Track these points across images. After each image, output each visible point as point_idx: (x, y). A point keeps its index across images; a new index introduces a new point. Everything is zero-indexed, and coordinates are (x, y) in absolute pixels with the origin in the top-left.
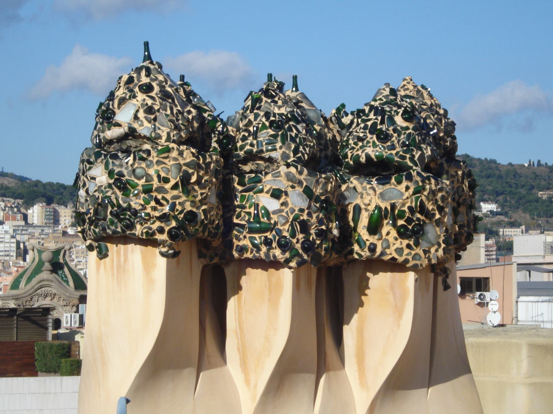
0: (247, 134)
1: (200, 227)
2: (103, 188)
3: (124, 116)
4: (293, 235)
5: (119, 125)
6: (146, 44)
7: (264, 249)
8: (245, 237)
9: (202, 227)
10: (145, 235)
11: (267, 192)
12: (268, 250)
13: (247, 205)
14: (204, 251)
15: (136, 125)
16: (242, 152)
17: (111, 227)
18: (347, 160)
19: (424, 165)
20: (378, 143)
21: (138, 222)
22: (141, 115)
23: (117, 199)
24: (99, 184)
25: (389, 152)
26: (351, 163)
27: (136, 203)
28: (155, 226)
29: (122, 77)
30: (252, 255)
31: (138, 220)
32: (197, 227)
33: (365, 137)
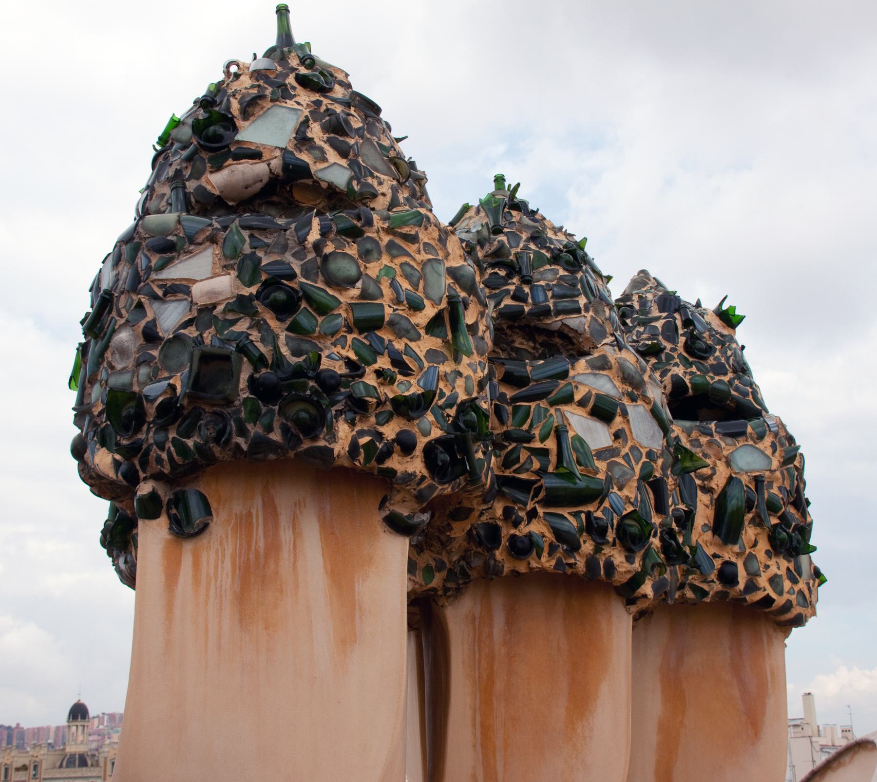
5: (256, 155)
7: (587, 547)
10: (361, 458)
11: (582, 403)
12: (598, 549)
13: (536, 432)
17: (249, 426)
20: (691, 359)
21: (340, 413)
22: (315, 131)
23: (270, 338)
24: (202, 301)
27: (333, 359)
28: (390, 431)
30: (553, 563)
31: (339, 407)
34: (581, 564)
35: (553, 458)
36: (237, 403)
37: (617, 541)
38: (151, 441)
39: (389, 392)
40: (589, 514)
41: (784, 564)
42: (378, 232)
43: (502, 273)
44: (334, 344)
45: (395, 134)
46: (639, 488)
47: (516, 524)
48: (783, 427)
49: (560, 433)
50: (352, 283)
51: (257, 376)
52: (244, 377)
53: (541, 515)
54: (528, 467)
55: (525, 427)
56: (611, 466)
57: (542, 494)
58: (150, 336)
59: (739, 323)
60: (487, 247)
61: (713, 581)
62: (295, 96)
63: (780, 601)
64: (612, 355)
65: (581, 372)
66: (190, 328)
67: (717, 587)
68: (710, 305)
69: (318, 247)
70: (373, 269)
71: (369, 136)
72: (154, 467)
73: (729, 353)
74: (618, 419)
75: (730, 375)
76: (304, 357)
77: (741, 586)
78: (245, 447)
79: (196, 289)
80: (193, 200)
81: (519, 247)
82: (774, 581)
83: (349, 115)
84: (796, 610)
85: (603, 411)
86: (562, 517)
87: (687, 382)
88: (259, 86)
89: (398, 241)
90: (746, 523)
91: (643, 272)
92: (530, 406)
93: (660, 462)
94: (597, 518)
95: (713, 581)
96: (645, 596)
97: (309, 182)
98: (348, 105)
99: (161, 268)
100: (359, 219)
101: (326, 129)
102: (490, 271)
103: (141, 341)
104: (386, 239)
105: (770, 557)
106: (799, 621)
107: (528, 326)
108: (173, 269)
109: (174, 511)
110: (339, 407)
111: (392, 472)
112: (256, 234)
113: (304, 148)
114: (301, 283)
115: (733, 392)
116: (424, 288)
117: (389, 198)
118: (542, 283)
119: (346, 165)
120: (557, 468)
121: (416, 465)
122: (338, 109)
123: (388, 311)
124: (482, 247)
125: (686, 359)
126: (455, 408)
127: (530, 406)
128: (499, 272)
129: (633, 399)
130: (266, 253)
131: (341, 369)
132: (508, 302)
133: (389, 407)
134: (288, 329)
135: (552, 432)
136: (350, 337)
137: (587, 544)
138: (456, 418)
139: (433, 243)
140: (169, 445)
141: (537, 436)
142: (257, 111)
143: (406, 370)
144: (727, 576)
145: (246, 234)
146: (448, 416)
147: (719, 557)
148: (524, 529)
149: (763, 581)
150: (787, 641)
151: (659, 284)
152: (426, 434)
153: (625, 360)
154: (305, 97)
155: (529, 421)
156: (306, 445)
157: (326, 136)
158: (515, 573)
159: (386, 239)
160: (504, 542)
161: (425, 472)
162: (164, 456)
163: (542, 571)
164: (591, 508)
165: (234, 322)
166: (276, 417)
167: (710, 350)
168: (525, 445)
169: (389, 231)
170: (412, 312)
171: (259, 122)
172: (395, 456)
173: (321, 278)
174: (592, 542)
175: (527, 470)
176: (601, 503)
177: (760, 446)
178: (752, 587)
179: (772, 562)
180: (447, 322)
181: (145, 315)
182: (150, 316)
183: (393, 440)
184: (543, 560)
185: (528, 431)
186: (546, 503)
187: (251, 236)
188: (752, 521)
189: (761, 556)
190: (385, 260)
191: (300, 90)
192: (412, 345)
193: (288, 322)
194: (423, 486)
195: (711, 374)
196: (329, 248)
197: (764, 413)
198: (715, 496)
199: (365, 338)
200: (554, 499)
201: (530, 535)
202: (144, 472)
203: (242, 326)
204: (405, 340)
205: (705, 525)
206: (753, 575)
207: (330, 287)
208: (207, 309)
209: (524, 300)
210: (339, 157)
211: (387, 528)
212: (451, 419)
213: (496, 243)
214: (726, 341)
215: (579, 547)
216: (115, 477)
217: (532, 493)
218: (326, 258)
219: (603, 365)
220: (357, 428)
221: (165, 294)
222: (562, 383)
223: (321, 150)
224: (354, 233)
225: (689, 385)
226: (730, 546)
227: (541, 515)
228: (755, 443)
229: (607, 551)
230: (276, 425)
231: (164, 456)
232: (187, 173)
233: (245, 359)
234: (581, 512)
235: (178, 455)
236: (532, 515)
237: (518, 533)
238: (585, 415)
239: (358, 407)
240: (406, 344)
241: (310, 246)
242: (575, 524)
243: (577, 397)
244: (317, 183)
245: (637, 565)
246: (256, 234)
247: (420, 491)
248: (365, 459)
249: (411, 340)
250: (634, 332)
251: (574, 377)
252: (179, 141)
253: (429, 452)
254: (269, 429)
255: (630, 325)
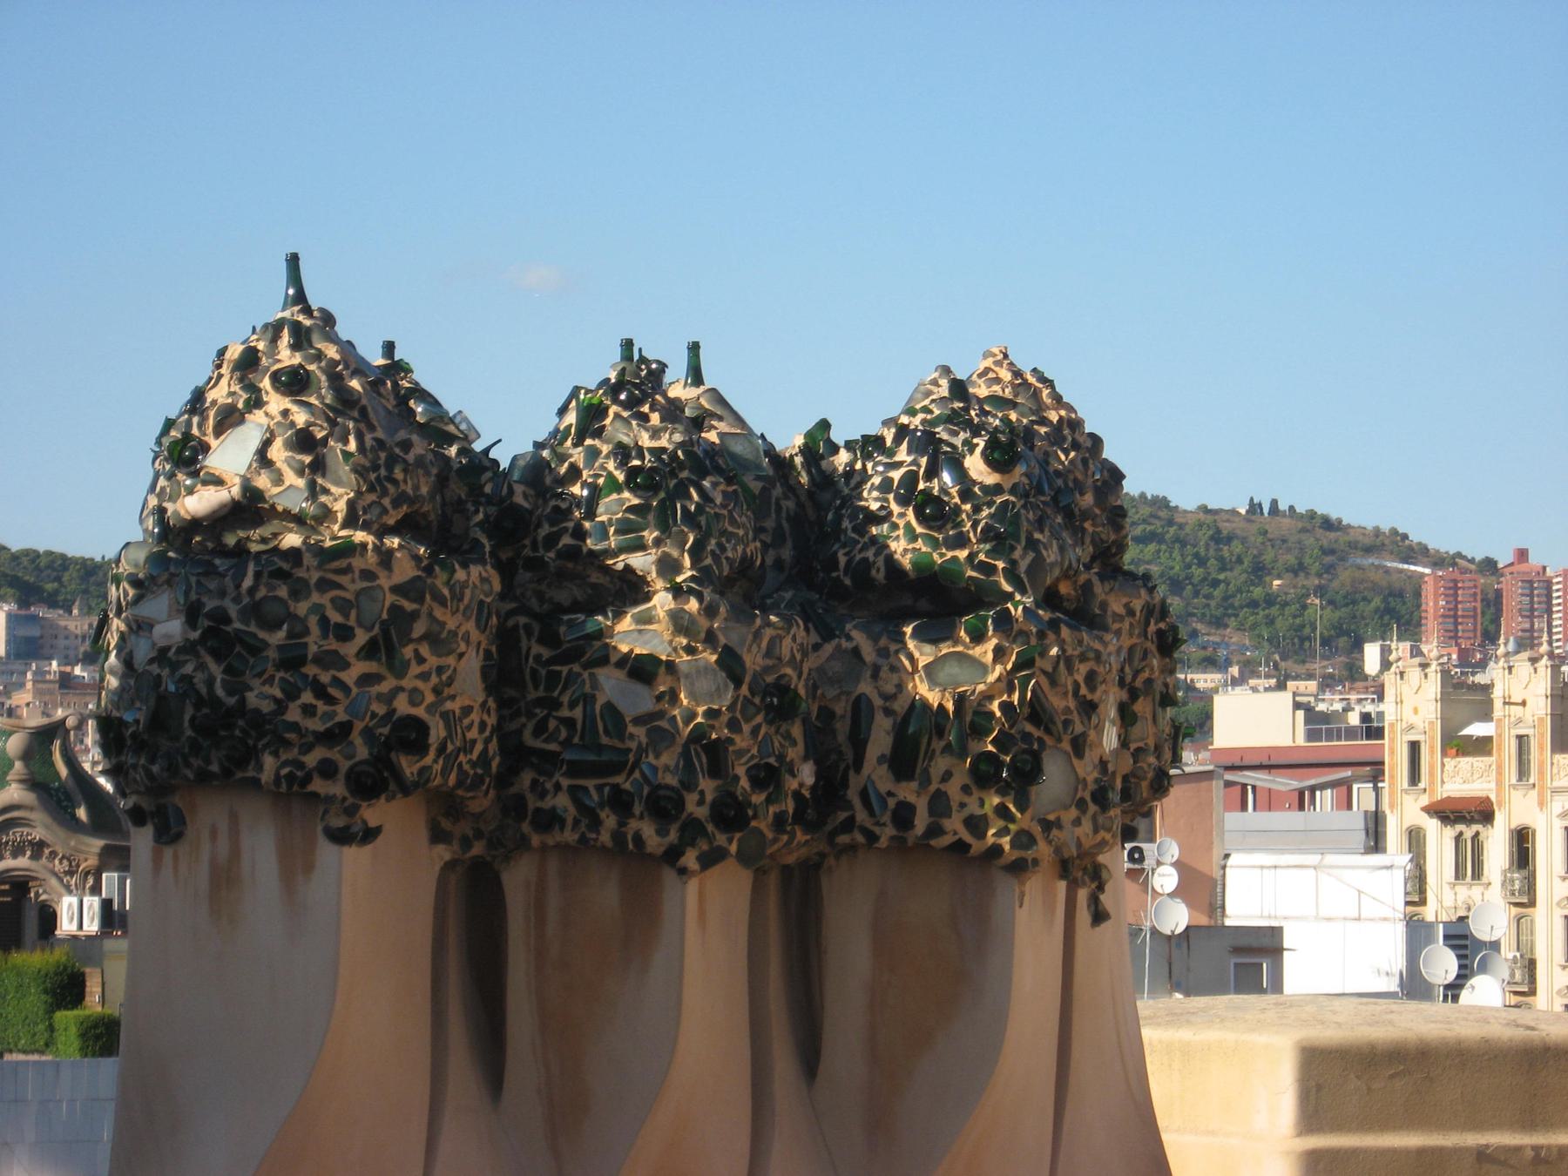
1: (435, 761)
2: (171, 654)
3: (231, 456)
4: (689, 784)
5: (218, 482)
6: (293, 261)
7: (610, 820)
8: (558, 787)
9: (441, 762)
10: (284, 785)
12: (622, 824)
13: (565, 699)
14: (446, 824)
15: (263, 481)
16: (552, 555)
17: (192, 760)
18: (834, 574)
19: (1043, 590)
20: (919, 530)
21: (265, 747)
22: (278, 452)
23: (210, 682)
24: (162, 643)
25: (950, 554)
26: (848, 582)
27: (261, 696)
28: (311, 760)
29: (226, 348)
30: (576, 837)
31: (265, 741)
32: (428, 760)
33: (883, 513)
39: (315, 725)
44: (264, 684)
70: (302, 608)
133: (311, 739)
148: (547, 803)
164: (618, 779)
190: (316, 598)
201: (554, 809)
208: (163, 651)
229: (633, 825)
245: (673, 836)
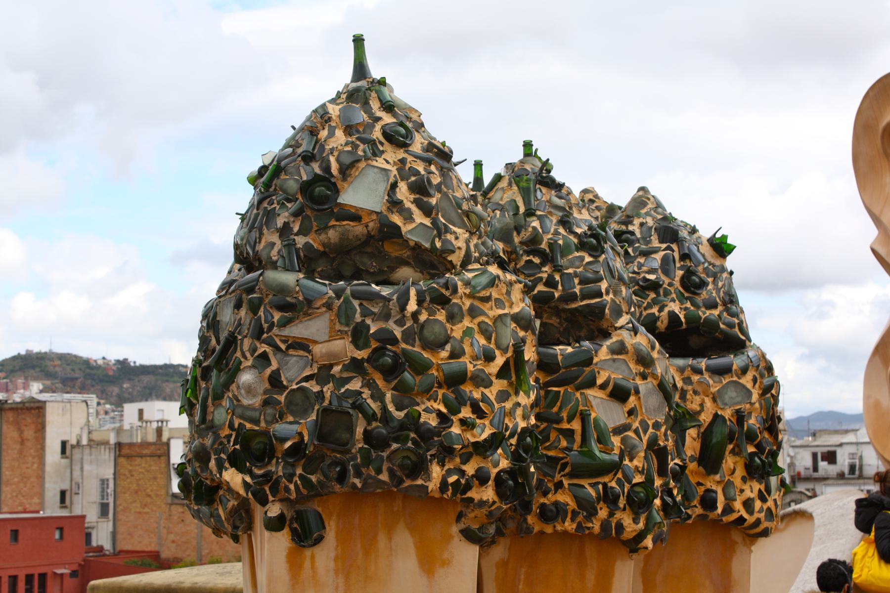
0: (537, 260)
6: (358, 41)
7: (603, 513)
10: (449, 493)
11: (603, 387)
12: (611, 514)
13: (564, 415)
17: (364, 470)
20: (686, 295)
22: (403, 192)
23: (378, 396)
28: (470, 469)
30: (574, 526)
31: (433, 452)
34: (596, 527)
35: (578, 438)
36: (353, 451)
37: (627, 507)
38: (281, 474)
40: (605, 485)
41: (757, 486)
42: (461, 298)
43: (537, 260)
44: (429, 400)
45: (454, 159)
46: (645, 458)
47: (545, 494)
48: (763, 356)
49: (584, 418)
50: (442, 346)
51: (369, 428)
52: (359, 431)
53: (567, 486)
54: (556, 444)
55: (555, 409)
56: (624, 441)
57: (568, 470)
58: (275, 381)
59: (730, 253)
60: (523, 233)
61: (695, 506)
62: (383, 152)
63: (750, 519)
64: (630, 340)
65: (603, 358)
66: (311, 382)
67: (699, 511)
68: (705, 233)
69: (415, 315)
70: (457, 332)
71: (445, 190)
72: (282, 494)
73: (720, 284)
74: (632, 399)
75: (720, 308)
76: (405, 411)
77: (719, 510)
78: (359, 485)
79: (317, 349)
80: (302, 254)
81: (550, 230)
82: (748, 504)
83: (431, 173)
84: (765, 525)
85: (619, 394)
86: (583, 487)
87: (682, 317)
88: (353, 143)
89: (477, 303)
90: (727, 453)
91: (642, 189)
92: (559, 392)
93: (663, 429)
94: (612, 488)
95: (695, 506)
96: (646, 548)
97: (400, 241)
98: (429, 162)
99: (284, 324)
100: (447, 289)
101: (412, 188)
102: (525, 258)
103: (267, 385)
104: (468, 303)
105: (745, 482)
106: (765, 533)
107: (556, 307)
108: (294, 328)
109: (295, 525)
110: (433, 452)
111: (471, 500)
112: (365, 303)
113: (395, 210)
114: (403, 349)
115: (722, 326)
116: (496, 340)
117: (463, 252)
118: (570, 271)
119: (429, 224)
120: (581, 447)
121: (488, 493)
122: (420, 167)
123: (470, 367)
124: (519, 233)
125: (683, 295)
126: (516, 437)
127: (559, 392)
128: (534, 260)
129: (644, 377)
130: (373, 320)
131: (433, 422)
132: (540, 288)
133: (471, 449)
134: (393, 389)
135: (578, 414)
136: (441, 392)
137: (603, 511)
138: (518, 445)
139: (502, 298)
140: (296, 479)
141: (565, 418)
142: (354, 172)
143: (481, 414)
144: (708, 502)
145: (356, 303)
146: (511, 445)
147: (702, 484)
148: (551, 498)
149: (738, 505)
150: (753, 548)
151: (658, 205)
152: (496, 464)
153: (639, 344)
154: (392, 155)
155: (559, 404)
156: (408, 483)
157: (412, 197)
158: (542, 533)
159: (468, 303)
160: (535, 508)
161: (496, 499)
162: (292, 487)
163: (565, 533)
164: (606, 479)
165: (348, 380)
166: (385, 463)
167: (703, 284)
168: (555, 426)
169: (470, 296)
170: (486, 363)
171: (356, 183)
172: (474, 489)
173: (417, 342)
174: (607, 510)
175: (556, 448)
176: (615, 475)
177: (743, 381)
178: (728, 510)
179: (746, 487)
180: (513, 370)
181: (270, 364)
182: (274, 365)
183: (473, 476)
184: (567, 524)
185: (558, 413)
186: (571, 476)
187: (361, 305)
188: (733, 452)
189: (737, 479)
190: (467, 323)
191: (387, 147)
192: (486, 391)
193: (393, 384)
194: (493, 508)
195: (703, 309)
196: (423, 317)
197: (747, 343)
198: (702, 430)
199: (452, 392)
200: (578, 472)
201: (556, 504)
202: (274, 496)
203: (355, 385)
204: (482, 389)
205: (692, 456)
206: (729, 499)
207: (424, 349)
209: (556, 288)
210: (423, 216)
211: (463, 538)
212: (513, 447)
213: (530, 229)
214: (718, 272)
215: (597, 513)
216: (245, 495)
217: (559, 467)
218: (422, 327)
219: (620, 349)
220: (446, 468)
221: (288, 348)
222: (587, 369)
223: (409, 211)
224: (442, 301)
225: (683, 320)
226: (712, 476)
227: (567, 486)
228: (739, 378)
229: (618, 515)
230: (384, 468)
231: (292, 487)
232: (296, 229)
233: (360, 415)
234: (598, 483)
235: (304, 487)
236: (559, 486)
237: (546, 501)
238: (604, 397)
239: (446, 452)
240: (482, 392)
241: (409, 315)
242: (594, 494)
243: (599, 381)
244: (406, 241)
245: (641, 525)
246: (365, 303)
247: (490, 512)
248: (452, 493)
249: (485, 388)
250: (636, 263)
251: (596, 364)
252: (285, 191)
253: (499, 482)
254: (379, 471)
255: (632, 254)
